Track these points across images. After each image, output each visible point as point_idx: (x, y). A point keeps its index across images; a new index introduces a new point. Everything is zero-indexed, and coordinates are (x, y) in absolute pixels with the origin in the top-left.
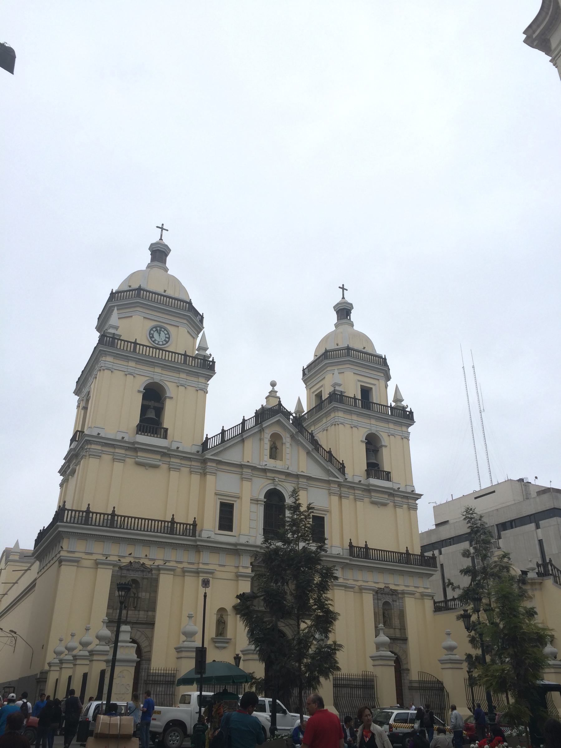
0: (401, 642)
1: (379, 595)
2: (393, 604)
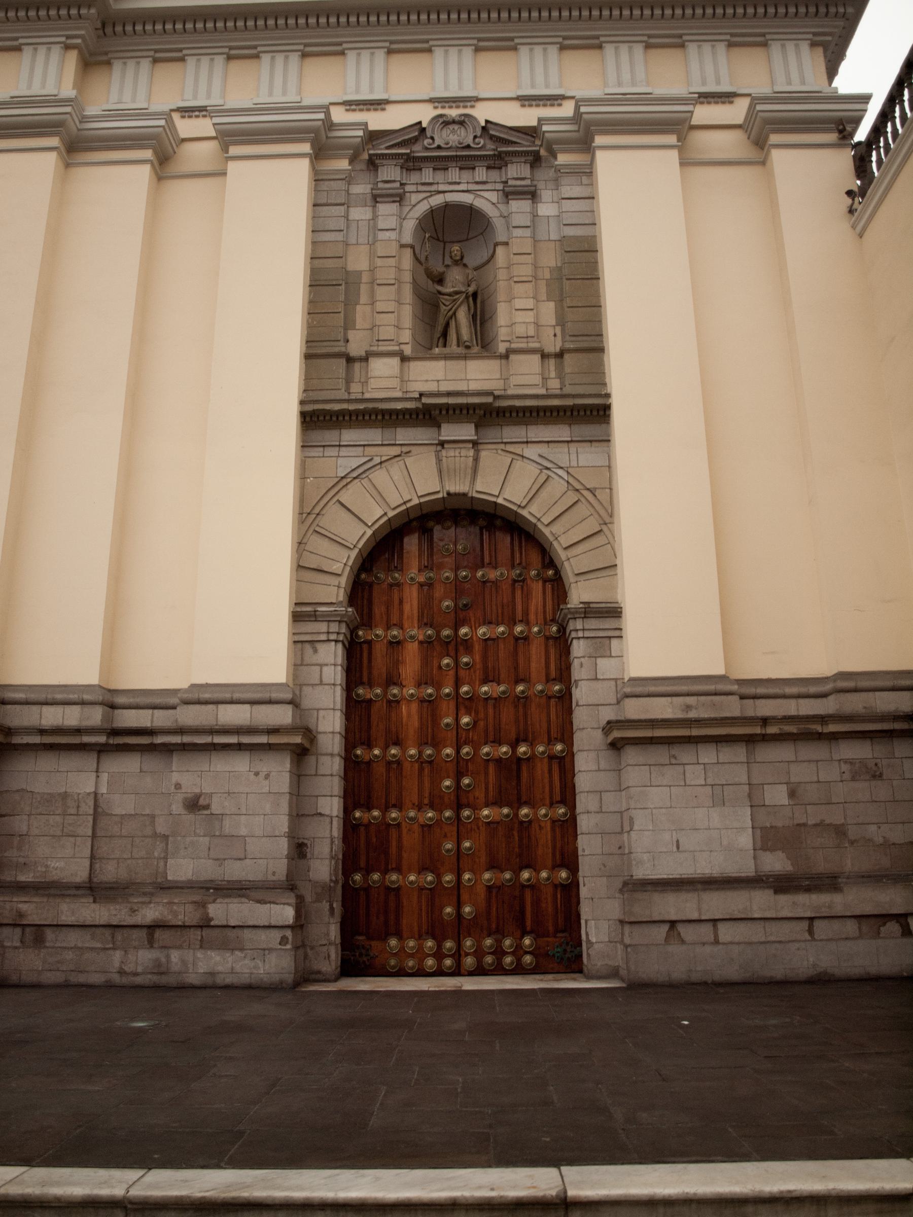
0: (562, 432)
1: (390, 172)
2: (506, 217)
